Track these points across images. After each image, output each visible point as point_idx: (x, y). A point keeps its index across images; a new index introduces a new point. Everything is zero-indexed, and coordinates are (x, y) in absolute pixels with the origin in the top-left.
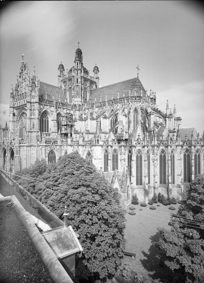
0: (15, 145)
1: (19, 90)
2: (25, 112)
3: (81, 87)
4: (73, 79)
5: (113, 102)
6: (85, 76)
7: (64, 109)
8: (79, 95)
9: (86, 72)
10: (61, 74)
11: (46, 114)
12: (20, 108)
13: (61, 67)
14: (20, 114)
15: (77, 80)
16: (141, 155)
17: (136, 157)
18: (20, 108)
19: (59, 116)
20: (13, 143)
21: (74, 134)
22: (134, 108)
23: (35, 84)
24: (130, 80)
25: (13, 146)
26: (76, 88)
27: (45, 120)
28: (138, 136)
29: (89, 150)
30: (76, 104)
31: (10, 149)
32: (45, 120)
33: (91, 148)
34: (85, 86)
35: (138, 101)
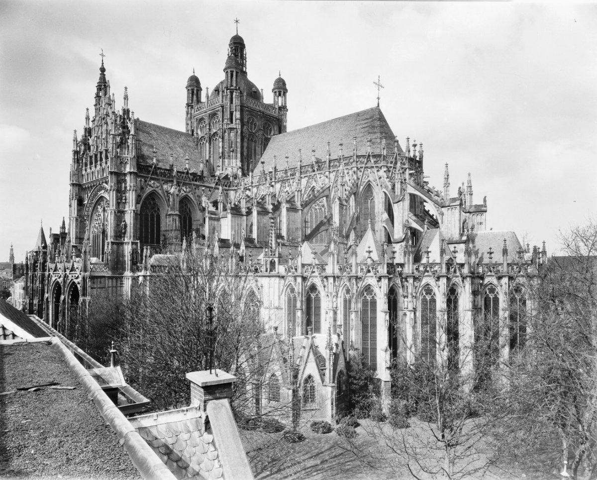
0: (80, 274)
1: (91, 142)
2: (106, 195)
3: (239, 132)
4: (220, 114)
5: (316, 170)
6: (251, 103)
7: (198, 186)
8: (237, 150)
9: (255, 94)
10: (192, 100)
11: (154, 199)
12: (94, 186)
13: (194, 85)
14: (94, 201)
15: (231, 114)
16: (373, 297)
17: (363, 302)
18: (94, 186)
19: (186, 205)
20: (77, 270)
21: (219, 247)
22: (365, 184)
23: (128, 128)
24: (358, 114)
25: (77, 275)
26: (229, 134)
27: (152, 215)
28: (367, 252)
29: (254, 286)
30: (227, 175)
31: (71, 283)
32: (152, 215)
33: (256, 281)
34: (251, 129)
35: (374, 165)
